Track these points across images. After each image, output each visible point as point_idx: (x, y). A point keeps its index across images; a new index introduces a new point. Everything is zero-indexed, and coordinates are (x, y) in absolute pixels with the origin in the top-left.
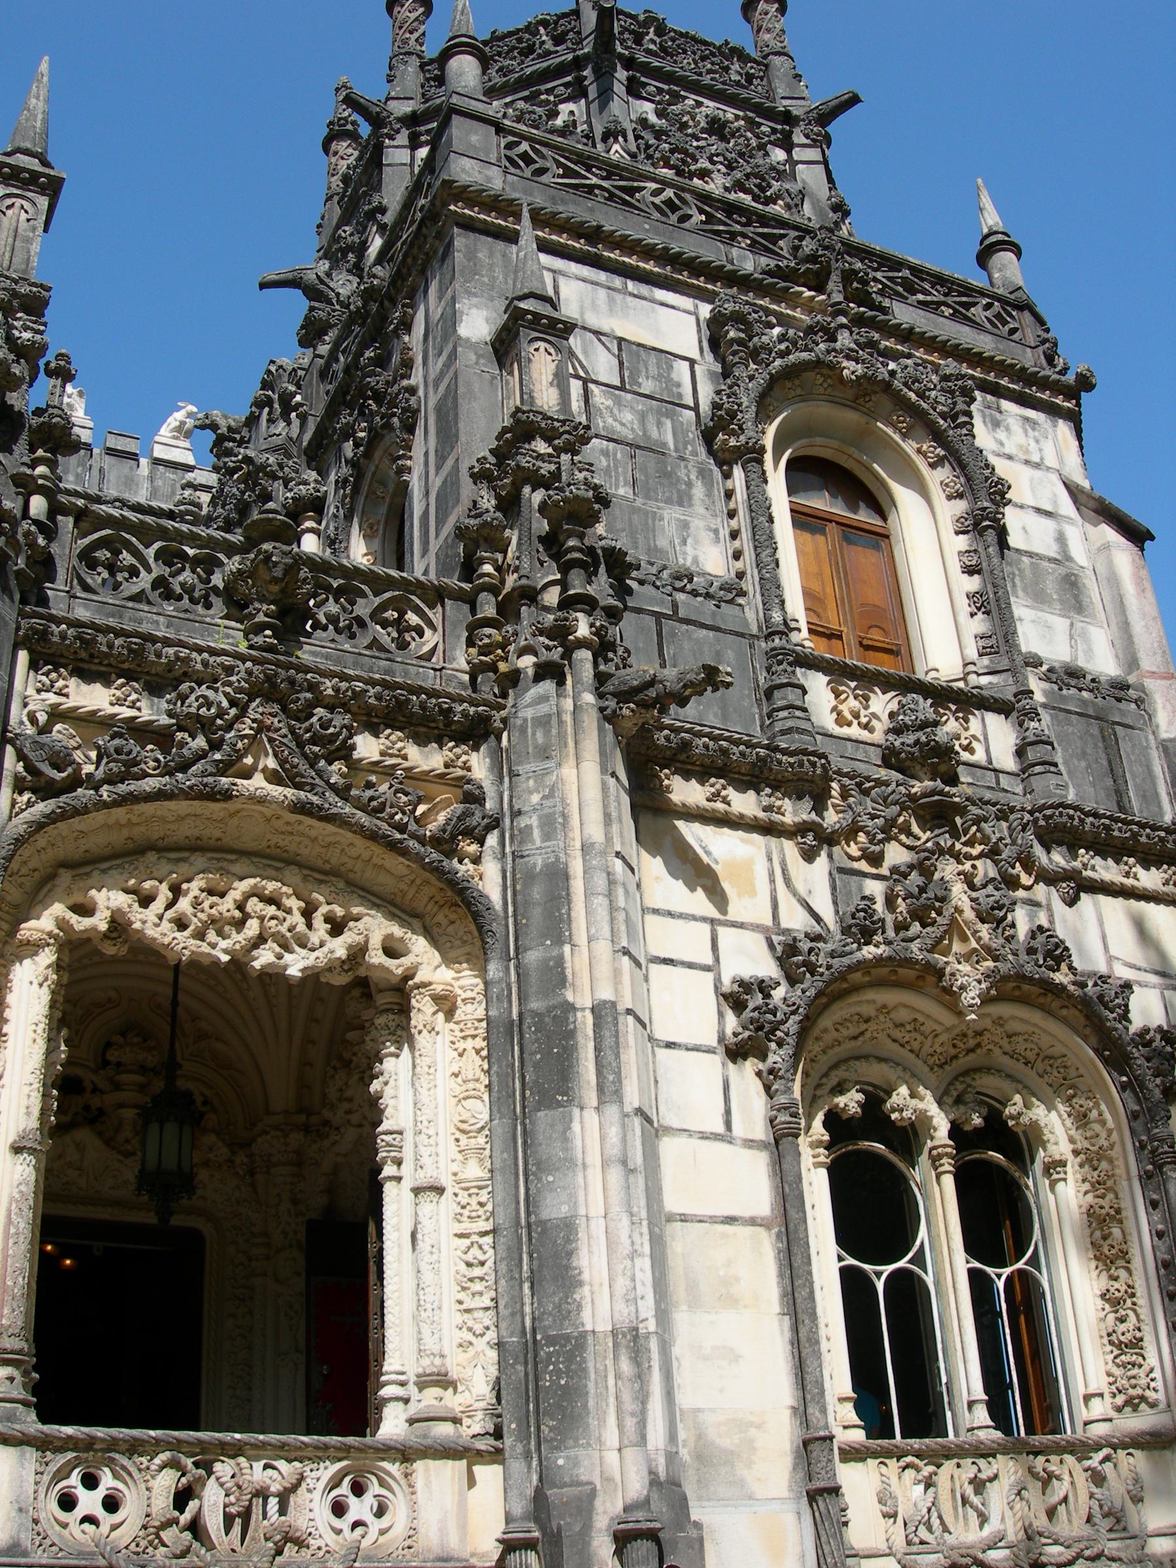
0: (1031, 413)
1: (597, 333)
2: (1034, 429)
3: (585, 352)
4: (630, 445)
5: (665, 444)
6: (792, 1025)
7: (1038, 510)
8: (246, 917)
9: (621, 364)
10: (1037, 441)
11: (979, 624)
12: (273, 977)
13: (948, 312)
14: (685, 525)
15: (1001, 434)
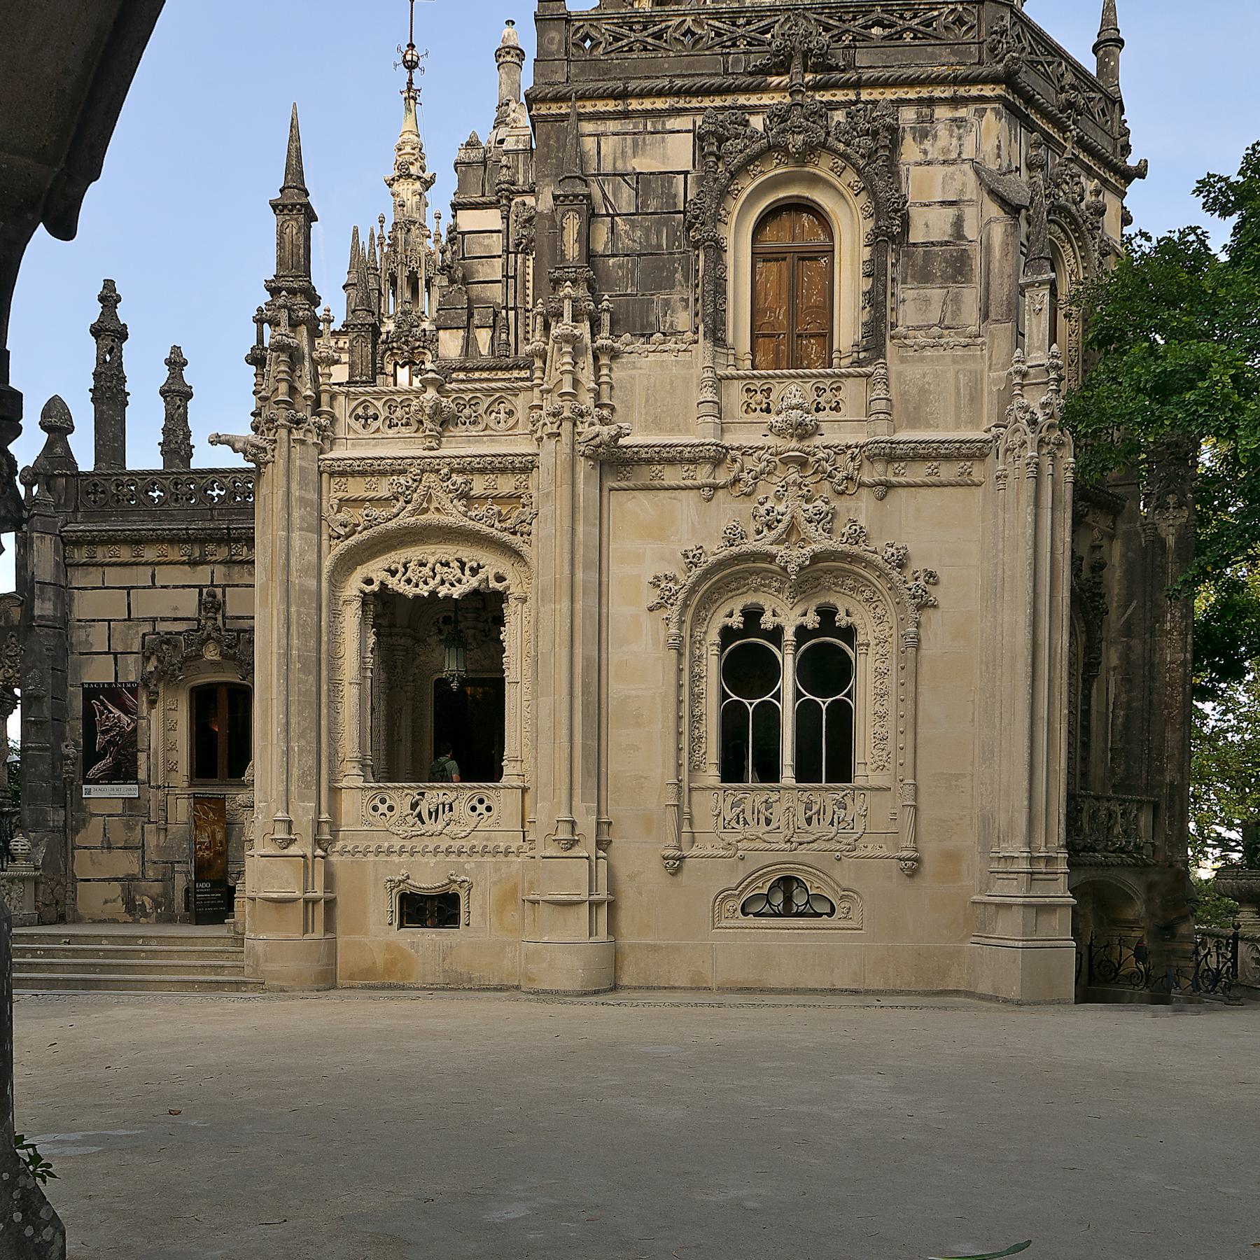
0: (962, 112)
1: (622, 175)
2: (959, 128)
3: (614, 195)
4: (638, 256)
5: (659, 246)
6: (681, 596)
7: (943, 203)
8: (435, 574)
9: (637, 194)
10: (960, 139)
11: (865, 316)
12: (448, 598)
13: (908, 36)
14: (667, 303)
15: (927, 144)
